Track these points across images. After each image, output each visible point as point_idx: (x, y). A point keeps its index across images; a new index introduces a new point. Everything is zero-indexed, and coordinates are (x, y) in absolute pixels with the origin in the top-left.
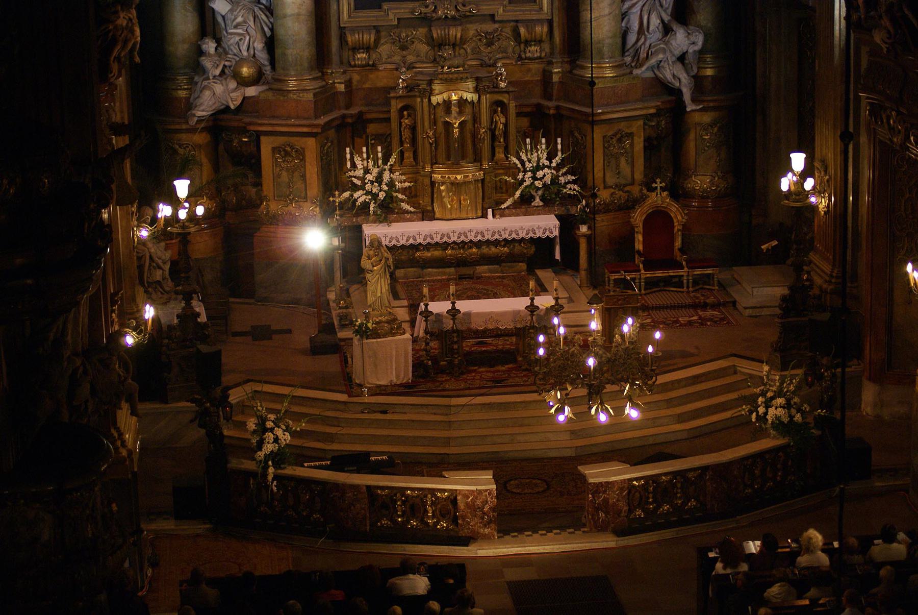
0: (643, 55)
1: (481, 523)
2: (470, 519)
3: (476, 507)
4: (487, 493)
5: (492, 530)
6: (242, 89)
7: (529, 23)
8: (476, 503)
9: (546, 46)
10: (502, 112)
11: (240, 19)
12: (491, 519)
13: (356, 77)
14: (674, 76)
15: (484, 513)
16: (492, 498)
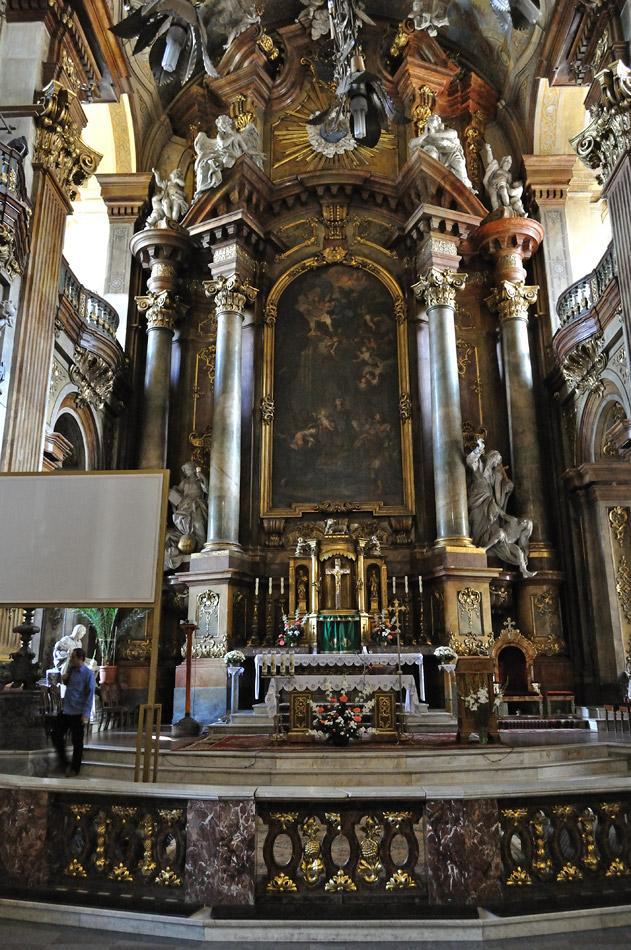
0: (486, 537)
1: (225, 871)
2: (206, 863)
3: (218, 836)
4: (238, 809)
5: (244, 887)
6: (181, 557)
7: (399, 518)
8: (217, 829)
9: (413, 536)
10: (376, 574)
11: (186, 506)
12: (243, 864)
13: (270, 555)
14: (512, 553)
15: (232, 851)
16: (247, 820)
